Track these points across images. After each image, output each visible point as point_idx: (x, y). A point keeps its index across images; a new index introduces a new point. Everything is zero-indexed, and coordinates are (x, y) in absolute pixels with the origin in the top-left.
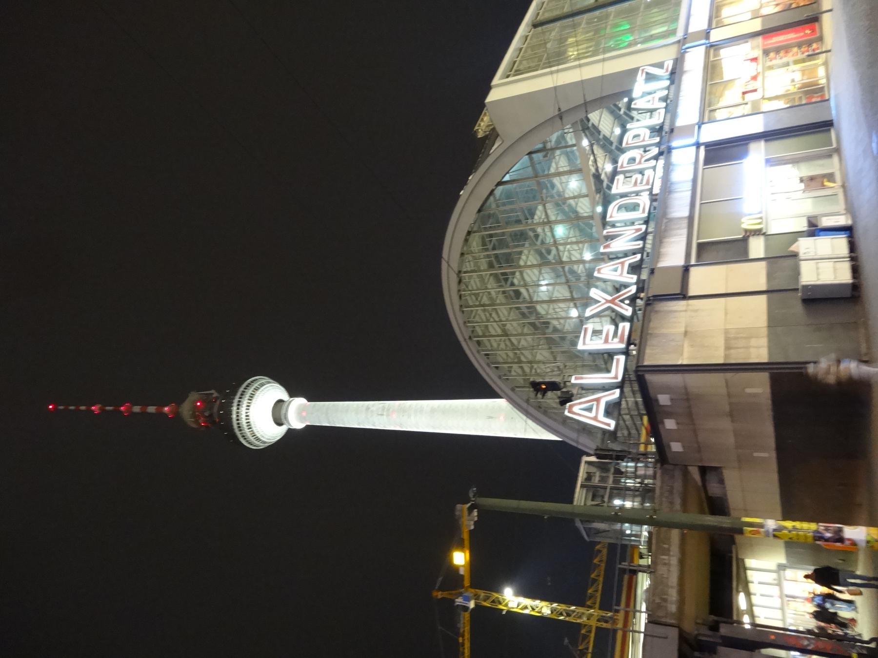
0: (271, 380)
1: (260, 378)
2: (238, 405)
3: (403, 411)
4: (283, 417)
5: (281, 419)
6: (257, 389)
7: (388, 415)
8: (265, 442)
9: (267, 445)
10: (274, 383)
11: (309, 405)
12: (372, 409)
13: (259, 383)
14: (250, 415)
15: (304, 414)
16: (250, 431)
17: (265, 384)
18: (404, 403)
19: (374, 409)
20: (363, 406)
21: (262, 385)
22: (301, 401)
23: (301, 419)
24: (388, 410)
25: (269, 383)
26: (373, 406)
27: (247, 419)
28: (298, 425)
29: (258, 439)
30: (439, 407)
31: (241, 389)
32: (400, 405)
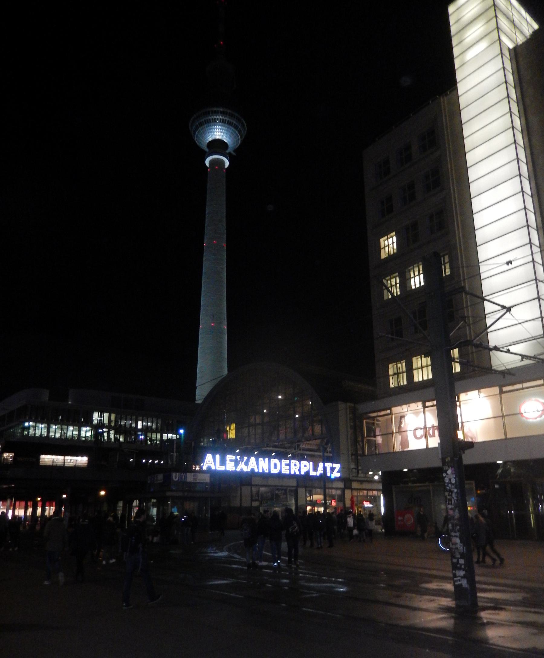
1: (245, 130)
6: (236, 127)
8: (195, 133)
10: (241, 141)
13: (241, 129)
14: (216, 123)
16: (203, 122)
21: (240, 132)
25: (241, 137)
27: (212, 119)
28: (207, 163)
29: (197, 128)
31: (236, 115)
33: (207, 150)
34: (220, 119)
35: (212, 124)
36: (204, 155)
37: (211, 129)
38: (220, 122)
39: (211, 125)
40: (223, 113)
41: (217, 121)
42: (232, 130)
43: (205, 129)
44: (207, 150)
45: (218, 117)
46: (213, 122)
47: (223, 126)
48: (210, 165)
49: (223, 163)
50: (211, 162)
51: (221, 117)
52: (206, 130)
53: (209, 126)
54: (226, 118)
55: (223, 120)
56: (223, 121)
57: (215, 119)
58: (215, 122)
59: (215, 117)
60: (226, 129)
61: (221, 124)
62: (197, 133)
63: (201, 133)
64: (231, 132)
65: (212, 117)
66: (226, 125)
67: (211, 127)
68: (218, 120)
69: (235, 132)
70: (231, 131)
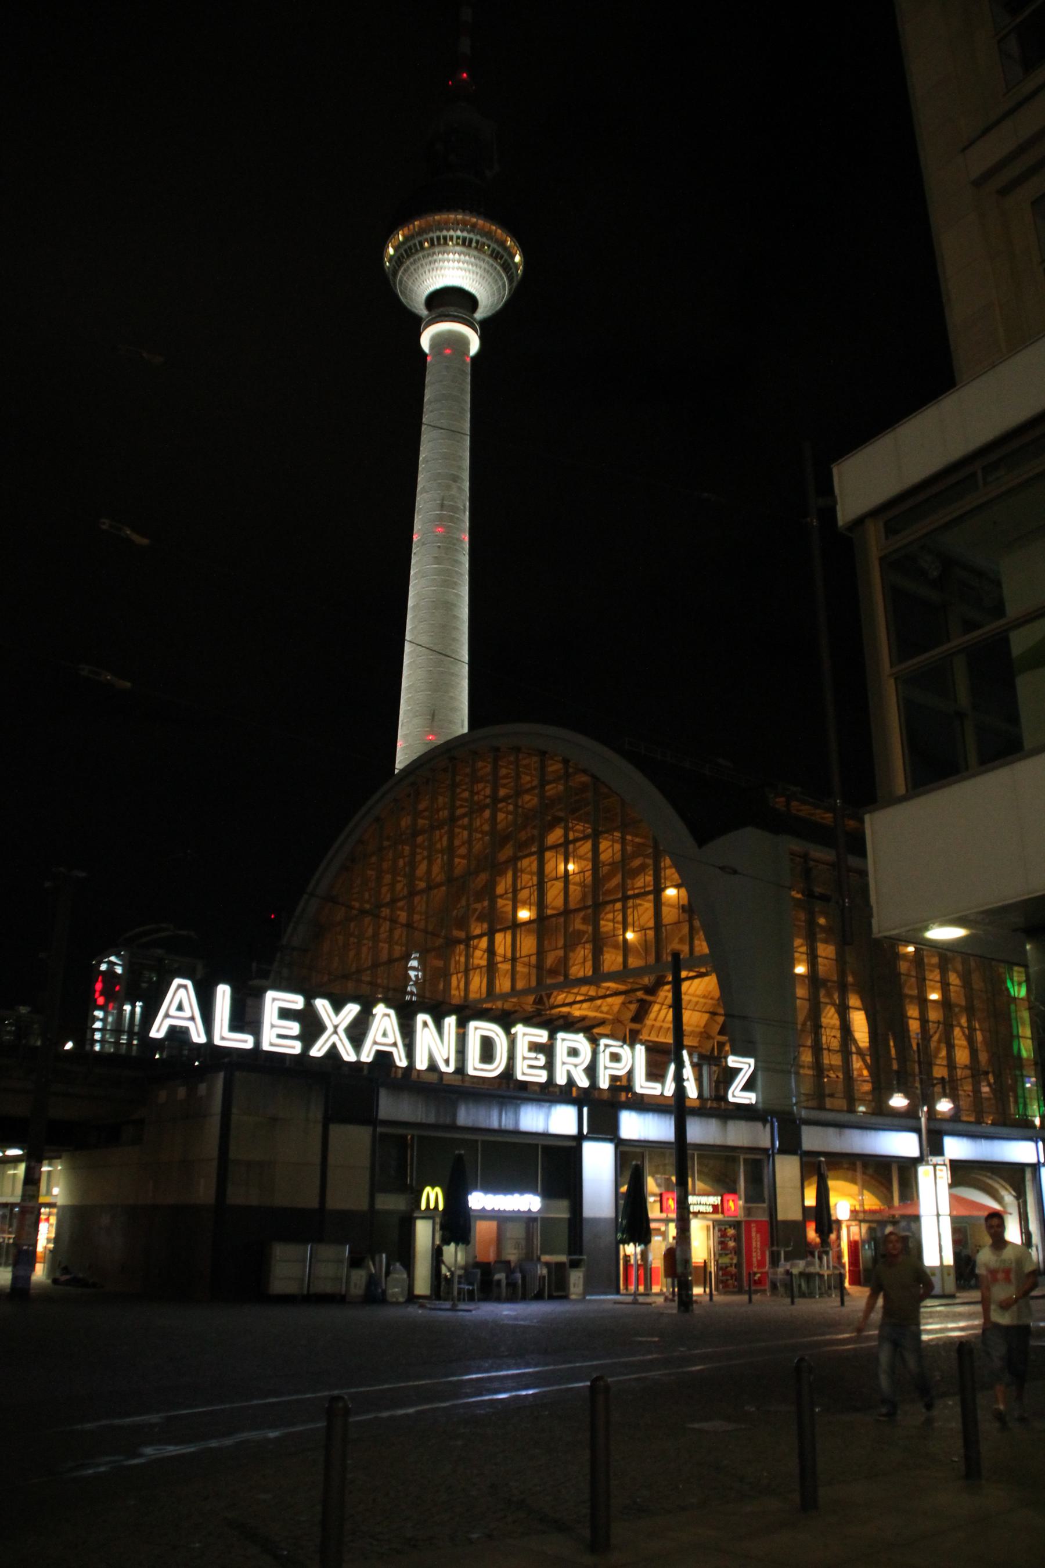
0: (515, 284)
2: (465, 223)
3: (449, 546)
4: (441, 310)
5: (442, 305)
7: (440, 518)
8: (395, 273)
9: (391, 277)
10: (510, 290)
11: (464, 361)
12: (454, 485)
15: (448, 352)
16: (415, 245)
17: (507, 273)
18: (463, 549)
19: (454, 491)
20: (460, 468)
22: (474, 345)
23: (441, 342)
24: (451, 519)
26: (460, 489)
27: (438, 238)
28: (425, 342)
30: (455, 617)
32: (462, 541)
33: (423, 312)
34: (458, 238)
35: (437, 250)
36: (416, 325)
37: (435, 261)
38: (458, 244)
39: (434, 253)
40: (464, 225)
41: (450, 243)
42: (488, 263)
43: (421, 262)
44: (423, 312)
45: (452, 233)
46: (439, 244)
47: (465, 255)
48: (432, 346)
49: (464, 342)
50: (438, 342)
51: (459, 233)
52: (422, 265)
53: (429, 255)
54: (472, 236)
55: (464, 239)
56: (466, 243)
57: (445, 238)
58: (446, 243)
59: (445, 233)
60: (473, 259)
61: (458, 248)
62: (400, 273)
63: (412, 273)
64: (485, 269)
65: (438, 233)
66: (475, 253)
67: (435, 257)
68: (451, 238)
69: (496, 268)
70: (483, 265)
